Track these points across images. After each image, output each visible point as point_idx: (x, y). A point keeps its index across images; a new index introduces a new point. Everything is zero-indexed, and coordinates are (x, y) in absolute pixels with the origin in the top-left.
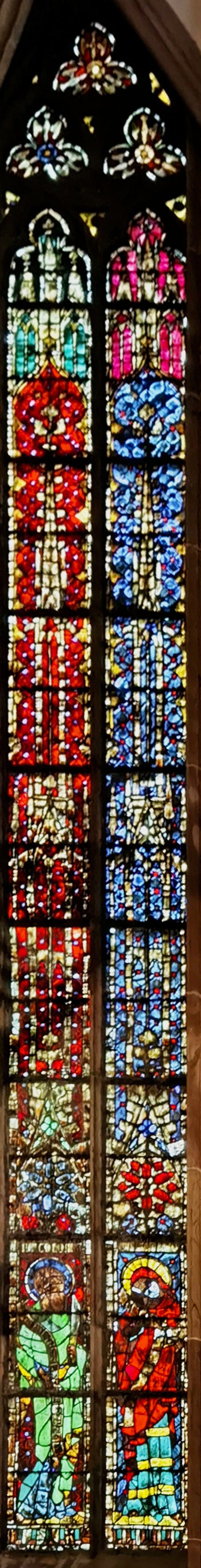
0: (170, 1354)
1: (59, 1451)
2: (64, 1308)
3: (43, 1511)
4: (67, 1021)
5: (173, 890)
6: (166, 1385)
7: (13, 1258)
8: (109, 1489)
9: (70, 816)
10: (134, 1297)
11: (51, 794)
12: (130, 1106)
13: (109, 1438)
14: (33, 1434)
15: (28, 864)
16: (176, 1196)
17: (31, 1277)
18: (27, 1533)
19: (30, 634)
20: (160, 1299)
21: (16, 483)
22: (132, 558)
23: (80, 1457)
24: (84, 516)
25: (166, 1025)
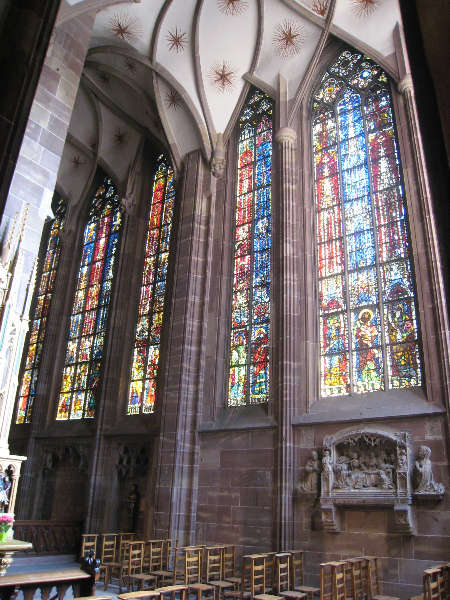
0: (265, 351)
1: (240, 380)
2: (242, 344)
3: (236, 396)
4: (245, 277)
5: (268, 241)
6: (264, 359)
7: (232, 334)
8: (251, 388)
9: (248, 233)
10: (257, 338)
11: (244, 229)
12: (258, 292)
13: (251, 375)
14: (235, 377)
15: (239, 245)
16: (267, 311)
17: (236, 338)
18: (232, 402)
19: (241, 199)
20: (263, 338)
21: (239, 172)
22: (260, 177)
23: (244, 381)
24: (252, 173)
25: (266, 272)
